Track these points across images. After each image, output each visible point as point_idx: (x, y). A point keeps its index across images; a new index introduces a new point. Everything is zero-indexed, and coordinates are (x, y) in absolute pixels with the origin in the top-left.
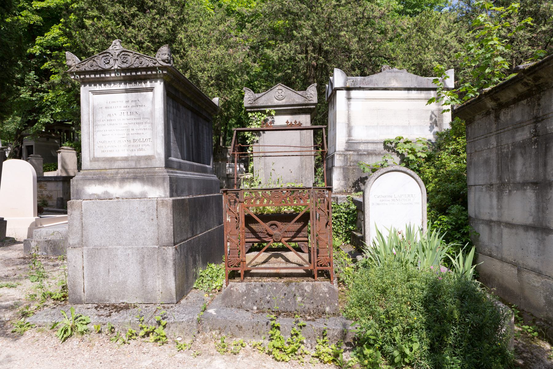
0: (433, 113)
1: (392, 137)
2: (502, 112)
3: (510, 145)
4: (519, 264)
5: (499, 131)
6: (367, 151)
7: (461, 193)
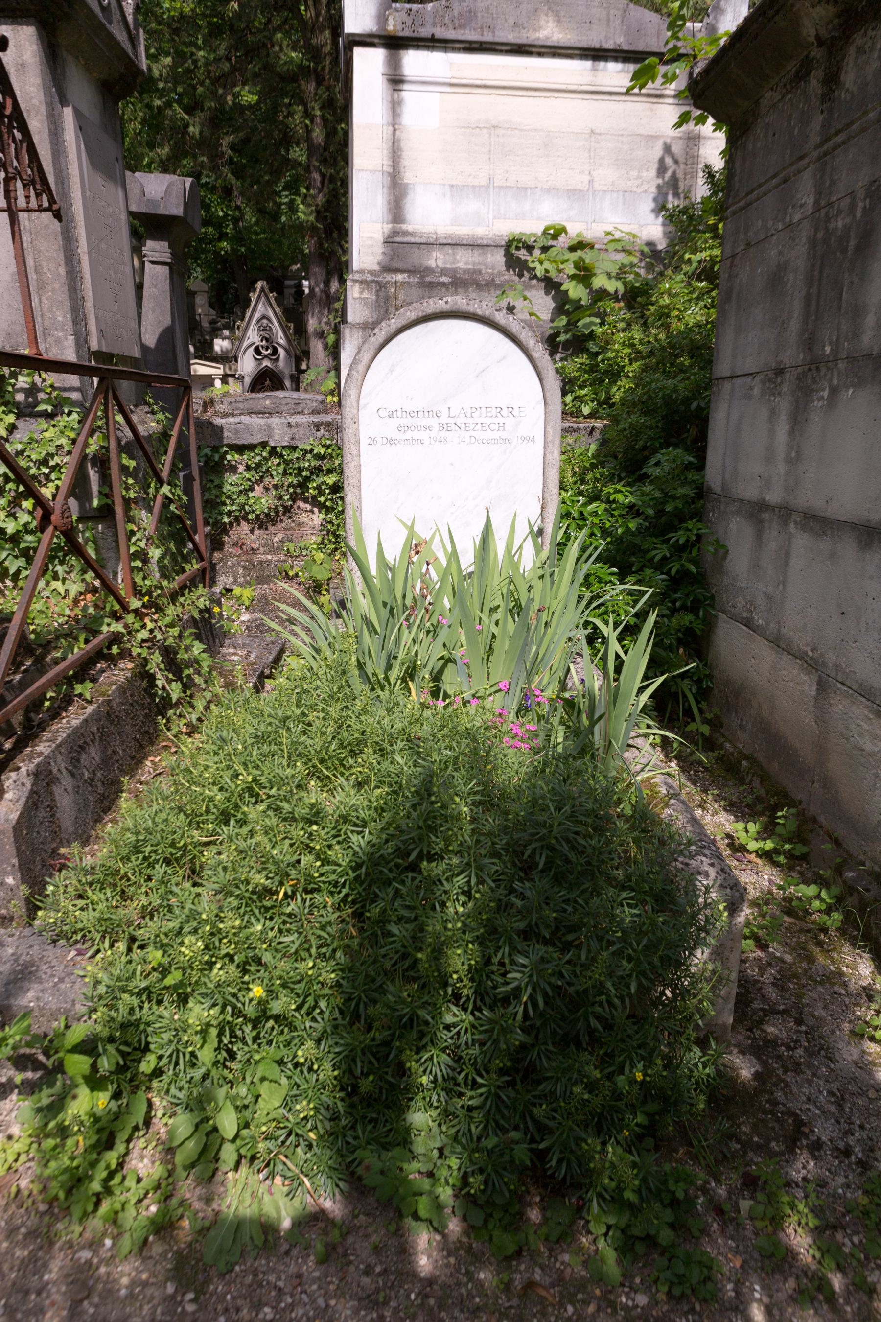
0: (667, 149)
1: (532, 226)
2: (852, 50)
3: (861, 194)
4: (824, 664)
5: (831, 144)
6: (452, 273)
7: (694, 405)
